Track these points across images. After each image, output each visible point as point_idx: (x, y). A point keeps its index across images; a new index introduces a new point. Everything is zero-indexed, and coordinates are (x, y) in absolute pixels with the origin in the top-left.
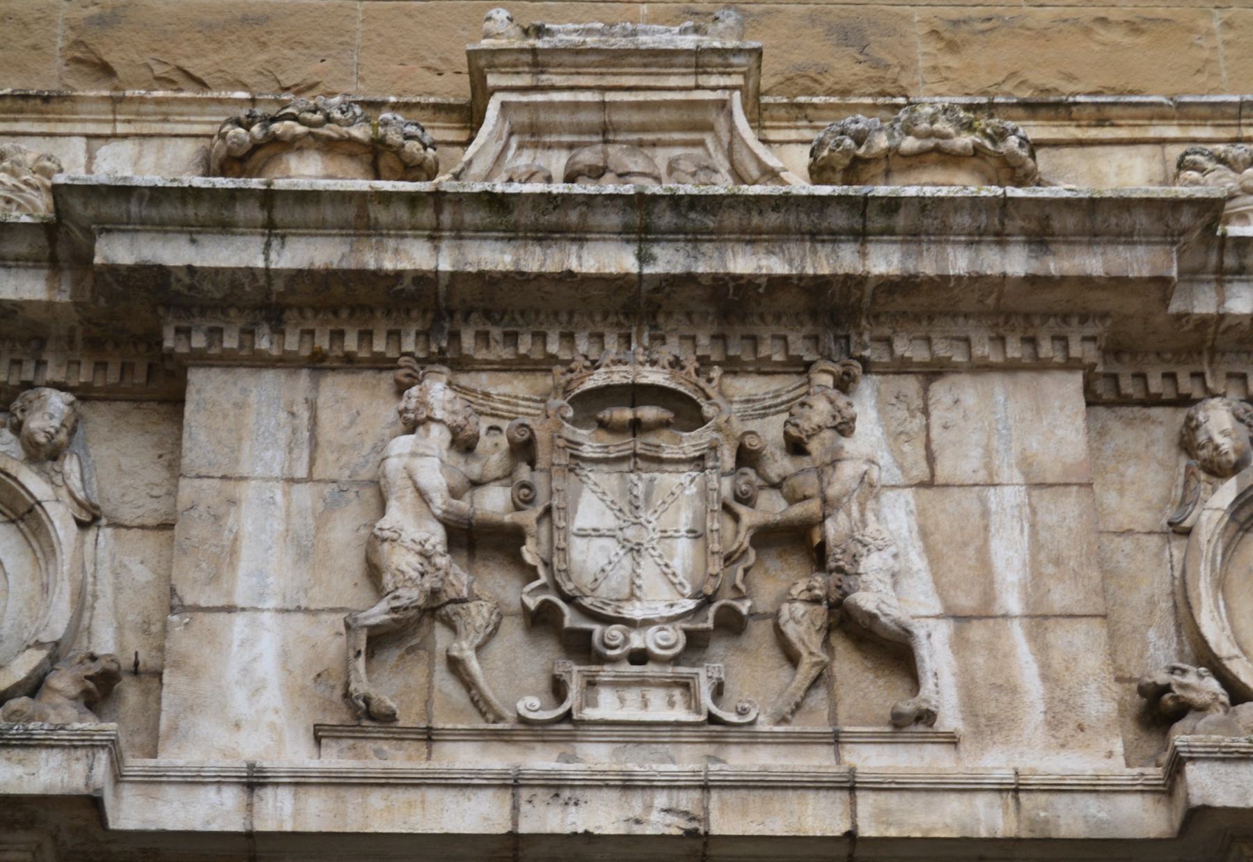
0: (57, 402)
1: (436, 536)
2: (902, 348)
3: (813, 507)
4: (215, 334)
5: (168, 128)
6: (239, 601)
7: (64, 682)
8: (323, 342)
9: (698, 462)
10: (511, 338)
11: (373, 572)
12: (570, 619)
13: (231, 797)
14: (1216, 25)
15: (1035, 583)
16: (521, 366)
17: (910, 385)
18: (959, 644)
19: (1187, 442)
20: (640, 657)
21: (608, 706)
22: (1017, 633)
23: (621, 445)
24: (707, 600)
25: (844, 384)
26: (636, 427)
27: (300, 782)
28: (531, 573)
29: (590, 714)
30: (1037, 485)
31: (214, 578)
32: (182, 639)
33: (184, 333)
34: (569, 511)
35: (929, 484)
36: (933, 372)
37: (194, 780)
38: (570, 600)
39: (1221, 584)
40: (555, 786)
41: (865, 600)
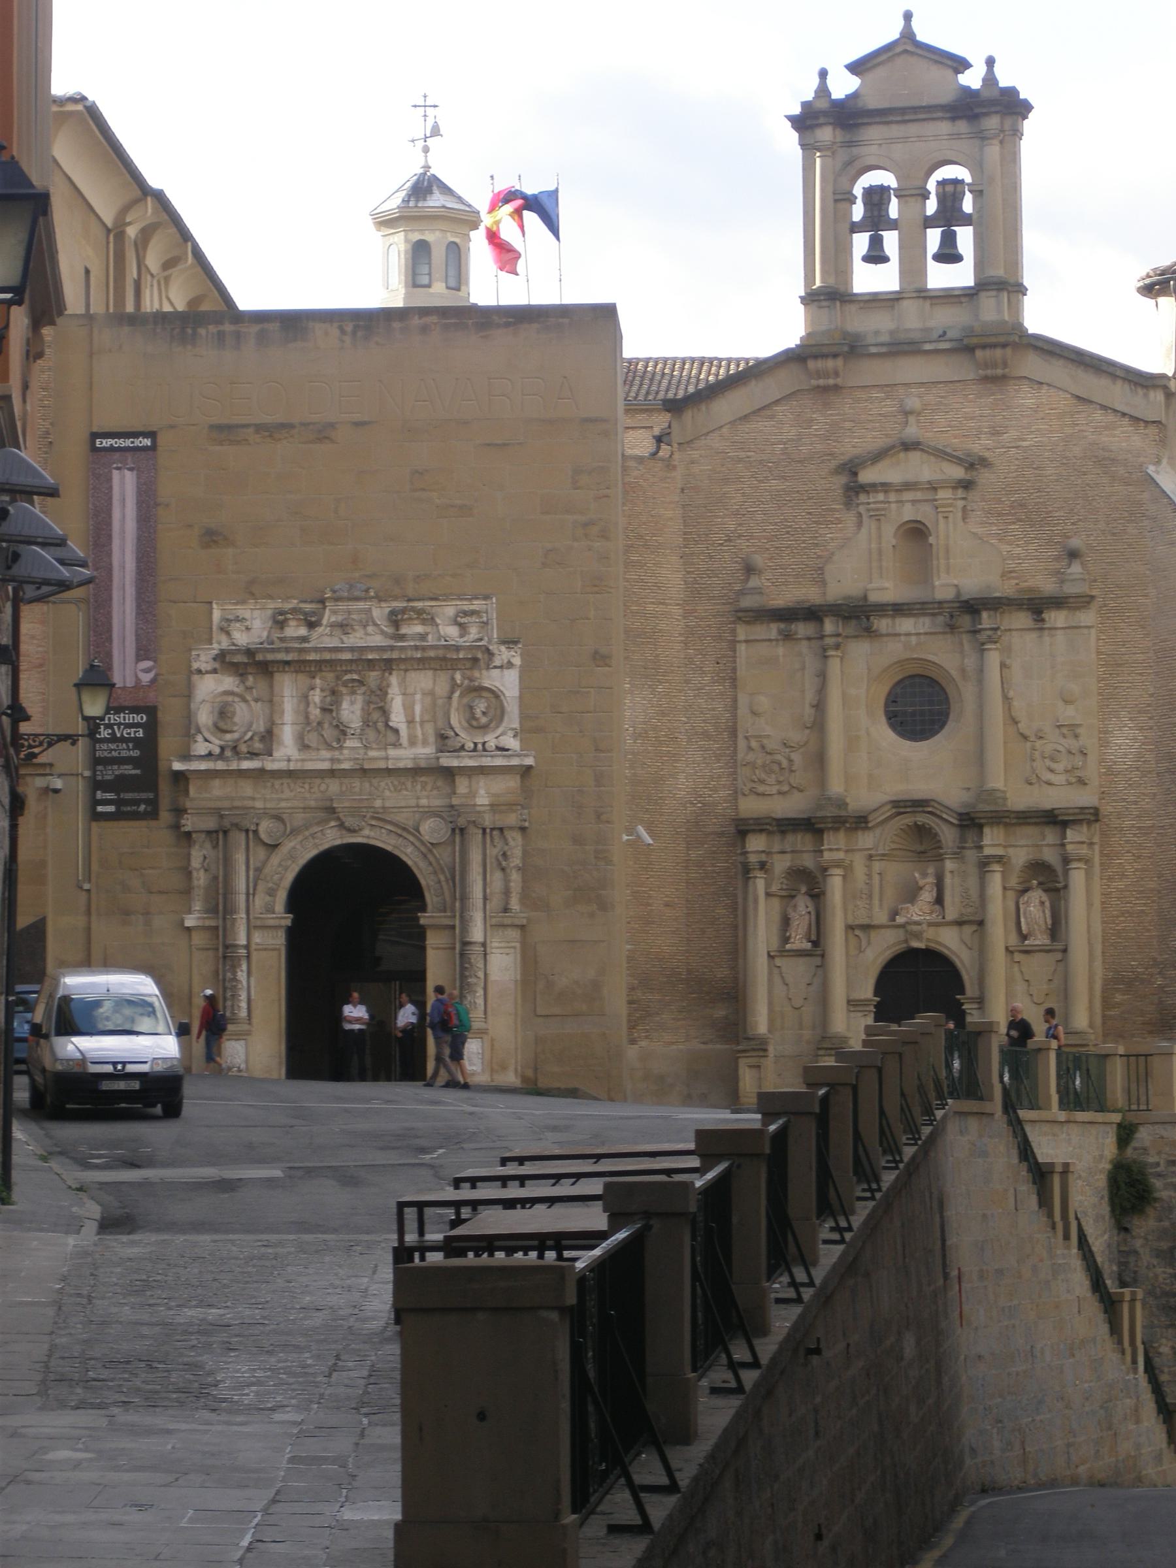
0: (251, 678)
4: (278, 668)
7: (256, 738)
12: (341, 728)
15: (422, 715)
18: (408, 727)
19: (453, 679)
21: (348, 744)
24: (364, 722)
25: (390, 674)
27: (297, 760)
30: (424, 694)
32: (275, 731)
34: (341, 705)
36: (406, 670)
37: (279, 761)
39: (457, 709)
41: (391, 724)
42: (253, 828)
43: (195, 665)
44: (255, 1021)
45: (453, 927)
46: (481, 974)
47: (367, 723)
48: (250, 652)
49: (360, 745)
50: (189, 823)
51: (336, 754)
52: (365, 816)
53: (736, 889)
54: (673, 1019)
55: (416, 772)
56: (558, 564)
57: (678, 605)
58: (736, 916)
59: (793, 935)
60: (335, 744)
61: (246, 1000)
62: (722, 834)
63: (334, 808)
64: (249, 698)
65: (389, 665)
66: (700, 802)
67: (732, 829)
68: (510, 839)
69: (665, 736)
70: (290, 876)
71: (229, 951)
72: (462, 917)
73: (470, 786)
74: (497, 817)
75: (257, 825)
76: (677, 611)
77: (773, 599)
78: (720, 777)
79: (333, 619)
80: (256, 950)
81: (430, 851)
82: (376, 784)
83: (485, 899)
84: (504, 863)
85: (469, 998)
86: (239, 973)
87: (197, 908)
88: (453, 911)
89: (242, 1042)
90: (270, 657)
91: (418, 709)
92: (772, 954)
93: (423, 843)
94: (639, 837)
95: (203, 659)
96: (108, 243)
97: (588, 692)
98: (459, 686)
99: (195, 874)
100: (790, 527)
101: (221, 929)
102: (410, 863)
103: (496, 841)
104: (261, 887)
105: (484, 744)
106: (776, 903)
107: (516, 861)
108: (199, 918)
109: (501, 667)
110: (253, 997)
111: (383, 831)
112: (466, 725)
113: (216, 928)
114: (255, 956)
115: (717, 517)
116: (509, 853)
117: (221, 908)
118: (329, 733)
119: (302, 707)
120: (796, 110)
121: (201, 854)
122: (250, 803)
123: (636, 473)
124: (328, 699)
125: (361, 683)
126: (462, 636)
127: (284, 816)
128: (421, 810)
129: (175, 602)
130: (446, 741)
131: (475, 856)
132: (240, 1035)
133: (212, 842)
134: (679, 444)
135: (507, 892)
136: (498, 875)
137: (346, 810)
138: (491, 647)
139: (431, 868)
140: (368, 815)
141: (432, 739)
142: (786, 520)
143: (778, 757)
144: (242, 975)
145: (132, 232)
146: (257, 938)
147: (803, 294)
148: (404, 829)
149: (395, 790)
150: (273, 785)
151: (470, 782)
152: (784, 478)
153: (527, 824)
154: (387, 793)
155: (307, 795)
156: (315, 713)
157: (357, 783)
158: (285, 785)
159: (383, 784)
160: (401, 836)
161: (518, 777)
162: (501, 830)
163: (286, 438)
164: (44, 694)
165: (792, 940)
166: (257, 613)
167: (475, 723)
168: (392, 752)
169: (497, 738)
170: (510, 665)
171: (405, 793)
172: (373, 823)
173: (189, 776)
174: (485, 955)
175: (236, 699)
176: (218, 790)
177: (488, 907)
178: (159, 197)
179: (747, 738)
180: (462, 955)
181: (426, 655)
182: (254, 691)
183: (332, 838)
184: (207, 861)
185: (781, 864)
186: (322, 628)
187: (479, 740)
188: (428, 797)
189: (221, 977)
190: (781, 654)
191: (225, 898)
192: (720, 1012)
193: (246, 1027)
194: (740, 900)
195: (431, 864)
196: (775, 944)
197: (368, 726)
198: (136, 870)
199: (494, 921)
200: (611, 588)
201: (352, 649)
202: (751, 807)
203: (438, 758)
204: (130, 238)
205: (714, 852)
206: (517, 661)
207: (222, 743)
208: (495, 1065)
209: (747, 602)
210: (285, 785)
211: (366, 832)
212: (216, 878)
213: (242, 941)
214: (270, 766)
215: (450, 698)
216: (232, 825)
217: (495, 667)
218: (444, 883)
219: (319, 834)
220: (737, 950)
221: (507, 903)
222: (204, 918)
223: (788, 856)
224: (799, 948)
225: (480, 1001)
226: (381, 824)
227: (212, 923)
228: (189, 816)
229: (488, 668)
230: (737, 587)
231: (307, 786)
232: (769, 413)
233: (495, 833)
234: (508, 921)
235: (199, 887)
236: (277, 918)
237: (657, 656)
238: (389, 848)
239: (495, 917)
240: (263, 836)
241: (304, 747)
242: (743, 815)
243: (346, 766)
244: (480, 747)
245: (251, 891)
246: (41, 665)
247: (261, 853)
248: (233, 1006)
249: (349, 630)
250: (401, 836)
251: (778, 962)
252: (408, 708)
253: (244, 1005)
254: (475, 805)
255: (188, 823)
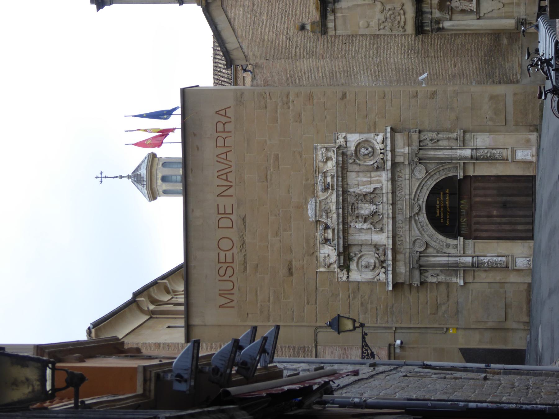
1: (365, 224)
2: (346, 187)
3: (362, 195)
5: (319, 247)
6: (370, 239)
7: (378, 252)
8: (346, 233)
9: (358, 204)
10: (345, 218)
11: (368, 229)
13: (389, 239)
14: (305, 156)
16: (348, 218)
17: (348, 186)
18: (373, 183)
19: (351, 163)
20: (376, 208)
21: (380, 211)
22: (372, 179)
23: (356, 210)
24: (371, 203)
25: (349, 192)
26: (355, 208)
27: (388, 234)
28: (369, 217)
29: (381, 212)
30: (358, 177)
31: (369, 241)
32: (374, 243)
33: (346, 244)
35: (358, 185)
36: (347, 184)
37: (388, 242)
38: (371, 214)
39: (365, 161)
40: (388, 215)
42: (418, 254)
43: (344, 279)
44: (506, 253)
45: (464, 163)
46: (486, 151)
47: (372, 202)
48: (339, 255)
49: (381, 205)
50: (416, 283)
51: (385, 216)
52: (413, 203)
53: (448, 34)
54: (508, 62)
55: (393, 180)
56: (300, 116)
57: (319, 62)
58: (461, 34)
59: (469, 8)
60: (381, 217)
61: (497, 258)
62: (423, 41)
63: (410, 217)
64: (359, 255)
65: (345, 192)
66: (408, 51)
67: (420, 36)
68: (424, 138)
69: (378, 67)
70: (441, 237)
71: (475, 265)
72: (460, 160)
73: (400, 156)
74: (414, 144)
75: (417, 252)
76: (321, 63)
77: (316, 18)
78: (396, 42)
79: (324, 217)
80: (474, 253)
81: (429, 174)
82: (399, 198)
83: (451, 149)
84: (435, 140)
85: (497, 156)
86: (485, 260)
87: (455, 279)
88: (457, 163)
89: (517, 259)
90: (341, 245)
91: (365, 179)
92: (478, 18)
93: (426, 177)
94: (424, 79)
95: (343, 276)
96: (157, 318)
97: (358, 102)
98: (354, 161)
99: (440, 280)
100: (283, 11)
101: (465, 269)
102: (435, 183)
103: (425, 144)
104: (445, 250)
105: (381, 149)
106: (454, 17)
107: (434, 135)
108: (460, 278)
109: (346, 142)
110: (496, 255)
111: (420, 195)
112: (372, 157)
113: (464, 271)
114: (477, 253)
115: (279, 44)
116: (431, 138)
117: (455, 269)
118: (376, 219)
119: (363, 231)
120: (94, 6)
121: (430, 277)
122: (407, 255)
123: (259, 81)
124: (360, 219)
125: (353, 204)
126: (332, 159)
127: (413, 240)
128: (411, 178)
129: (316, 289)
130: (379, 166)
131: (432, 153)
132: (513, 260)
133: (425, 273)
134: (246, 61)
135: (448, 139)
136: (440, 143)
137: (410, 212)
138: (337, 146)
139: (437, 174)
140: (413, 202)
141: (378, 173)
142: (280, 12)
143: (388, 15)
144: (486, 260)
145: (152, 307)
146: (469, 252)
147: (178, 4)
148: (419, 185)
149: (401, 189)
150: (399, 245)
151: (397, 156)
152: (261, 14)
153: (417, 130)
154: (403, 193)
155: (404, 229)
156: (365, 226)
157: (399, 206)
158: (399, 239)
159: (399, 195)
160: (422, 187)
161: (396, 134)
162: (420, 142)
163: (243, 238)
164: (358, 348)
165: (472, 8)
166: (322, 251)
167: (371, 154)
168: (384, 191)
169: (378, 144)
170: (345, 138)
171: (403, 185)
172: (416, 199)
173: (395, 282)
174: (477, 149)
175: (360, 261)
176: (402, 269)
177: (455, 148)
178: (136, 294)
179: (379, 30)
180: (477, 159)
181: (340, 176)
182: (356, 253)
183: (423, 218)
184: (434, 275)
185: (437, 14)
186: (328, 222)
187: (379, 151)
188: (405, 175)
189: (487, 269)
190: (340, 15)
191: (449, 267)
192: (505, 41)
193: (510, 258)
194: (453, 32)
195: (435, 174)
196: (474, 16)
197: (372, 202)
198: (438, 307)
199: (462, 145)
200: (311, 92)
201: (337, 209)
202: (410, 28)
203: (387, 170)
204: (154, 308)
205: (431, 45)
206: (344, 134)
207: (380, 267)
208: (527, 144)
209: (318, 29)
210: (399, 239)
211: (420, 202)
212: (441, 271)
213: (469, 260)
214: (391, 246)
215: (360, 165)
216: (417, 263)
217: (346, 144)
218: (444, 167)
219: (422, 224)
220: (476, 34)
221: (454, 139)
222: (460, 276)
223: (433, 10)
224: (476, 5)
225: (499, 151)
226: (417, 196)
227: (462, 272)
228: (413, 283)
229: (347, 147)
230: (311, 34)
231: (400, 229)
232: (232, 20)
233: (421, 144)
234: (462, 139)
235: (445, 278)
236: (460, 243)
237: (342, 71)
238: (428, 192)
239: (460, 145)
240: (422, 249)
241: (382, 230)
242: (414, 33)
243: (390, 212)
244: (382, 151)
245: (448, 255)
246: (345, 349)
247: (430, 250)
248: (500, 264)
249: (329, 211)
250: (422, 187)
251: (482, 15)
252: (365, 183)
253: (500, 259)
254: (409, 153)
255: (416, 282)
